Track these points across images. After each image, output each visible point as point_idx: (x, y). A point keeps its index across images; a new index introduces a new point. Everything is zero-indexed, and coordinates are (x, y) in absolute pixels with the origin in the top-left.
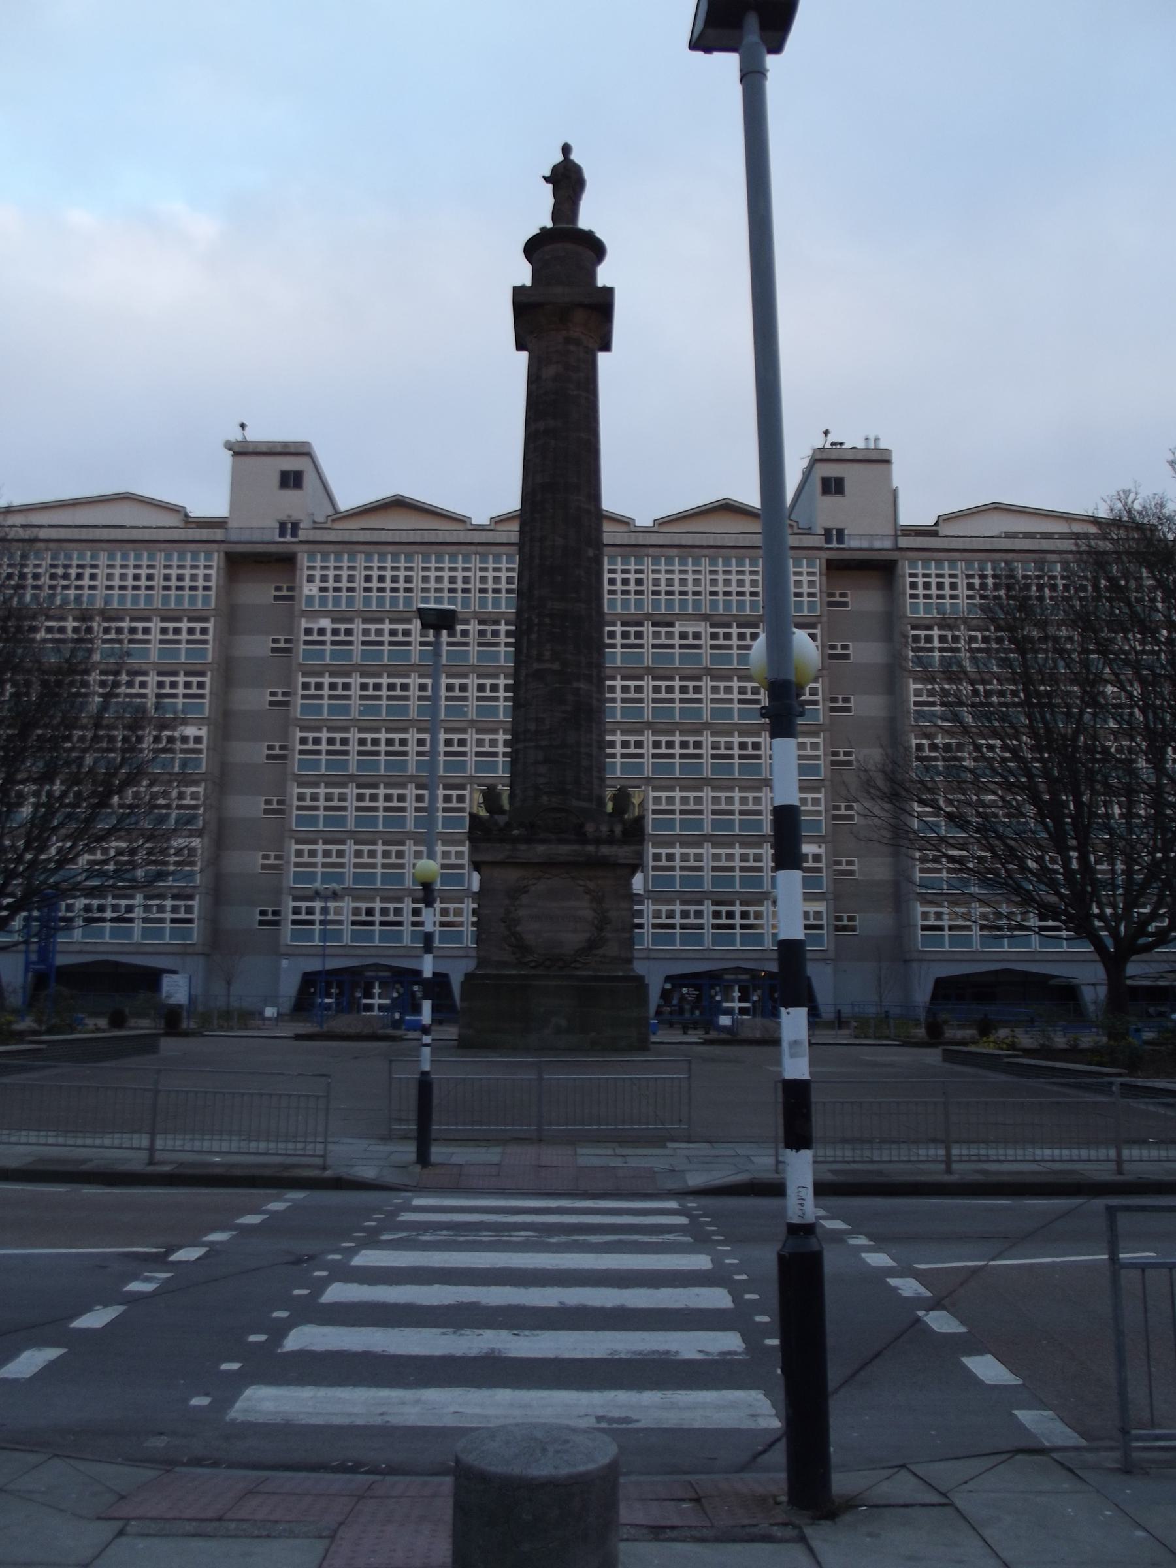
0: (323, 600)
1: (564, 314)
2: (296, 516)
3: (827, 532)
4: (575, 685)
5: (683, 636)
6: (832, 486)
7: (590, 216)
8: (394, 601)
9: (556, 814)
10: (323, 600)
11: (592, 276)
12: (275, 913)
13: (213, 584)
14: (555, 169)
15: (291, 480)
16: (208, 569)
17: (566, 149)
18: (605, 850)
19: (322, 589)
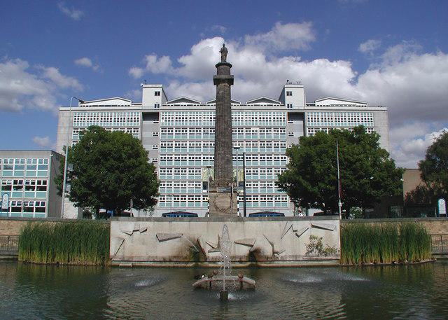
1: (223, 81)
5: (253, 131)
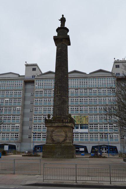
0: (38, 87)
1: (61, 40)
2: (35, 75)
3: (117, 74)
4: (63, 97)
6: (117, 66)
7: (66, 25)
8: (49, 87)
9: (61, 118)
10: (38, 87)
11: (67, 34)
12: (31, 136)
13: (22, 85)
14: (61, 18)
15: (34, 69)
16: (22, 82)
17: (63, 16)
18: (66, 124)
19: (38, 86)
